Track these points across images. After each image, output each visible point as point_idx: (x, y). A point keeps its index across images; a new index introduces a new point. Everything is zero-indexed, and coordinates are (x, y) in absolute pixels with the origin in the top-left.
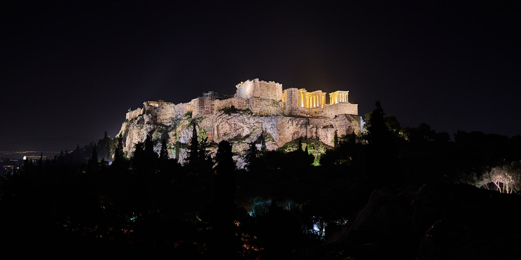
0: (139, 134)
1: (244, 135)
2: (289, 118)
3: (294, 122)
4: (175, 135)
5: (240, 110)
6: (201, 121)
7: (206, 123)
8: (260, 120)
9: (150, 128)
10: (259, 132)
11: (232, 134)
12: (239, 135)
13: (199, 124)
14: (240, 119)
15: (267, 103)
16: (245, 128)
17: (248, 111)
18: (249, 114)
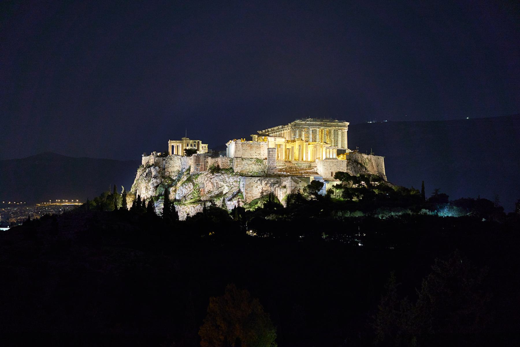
0: (147, 188)
1: (224, 192)
2: (257, 179)
3: (263, 181)
4: (175, 191)
5: (222, 170)
6: (197, 178)
7: (199, 180)
8: (238, 178)
9: (157, 182)
10: (235, 190)
11: (215, 192)
12: (222, 193)
13: (194, 181)
14: (220, 178)
15: (250, 162)
16: (225, 186)
17: (230, 170)
18: (231, 173)
